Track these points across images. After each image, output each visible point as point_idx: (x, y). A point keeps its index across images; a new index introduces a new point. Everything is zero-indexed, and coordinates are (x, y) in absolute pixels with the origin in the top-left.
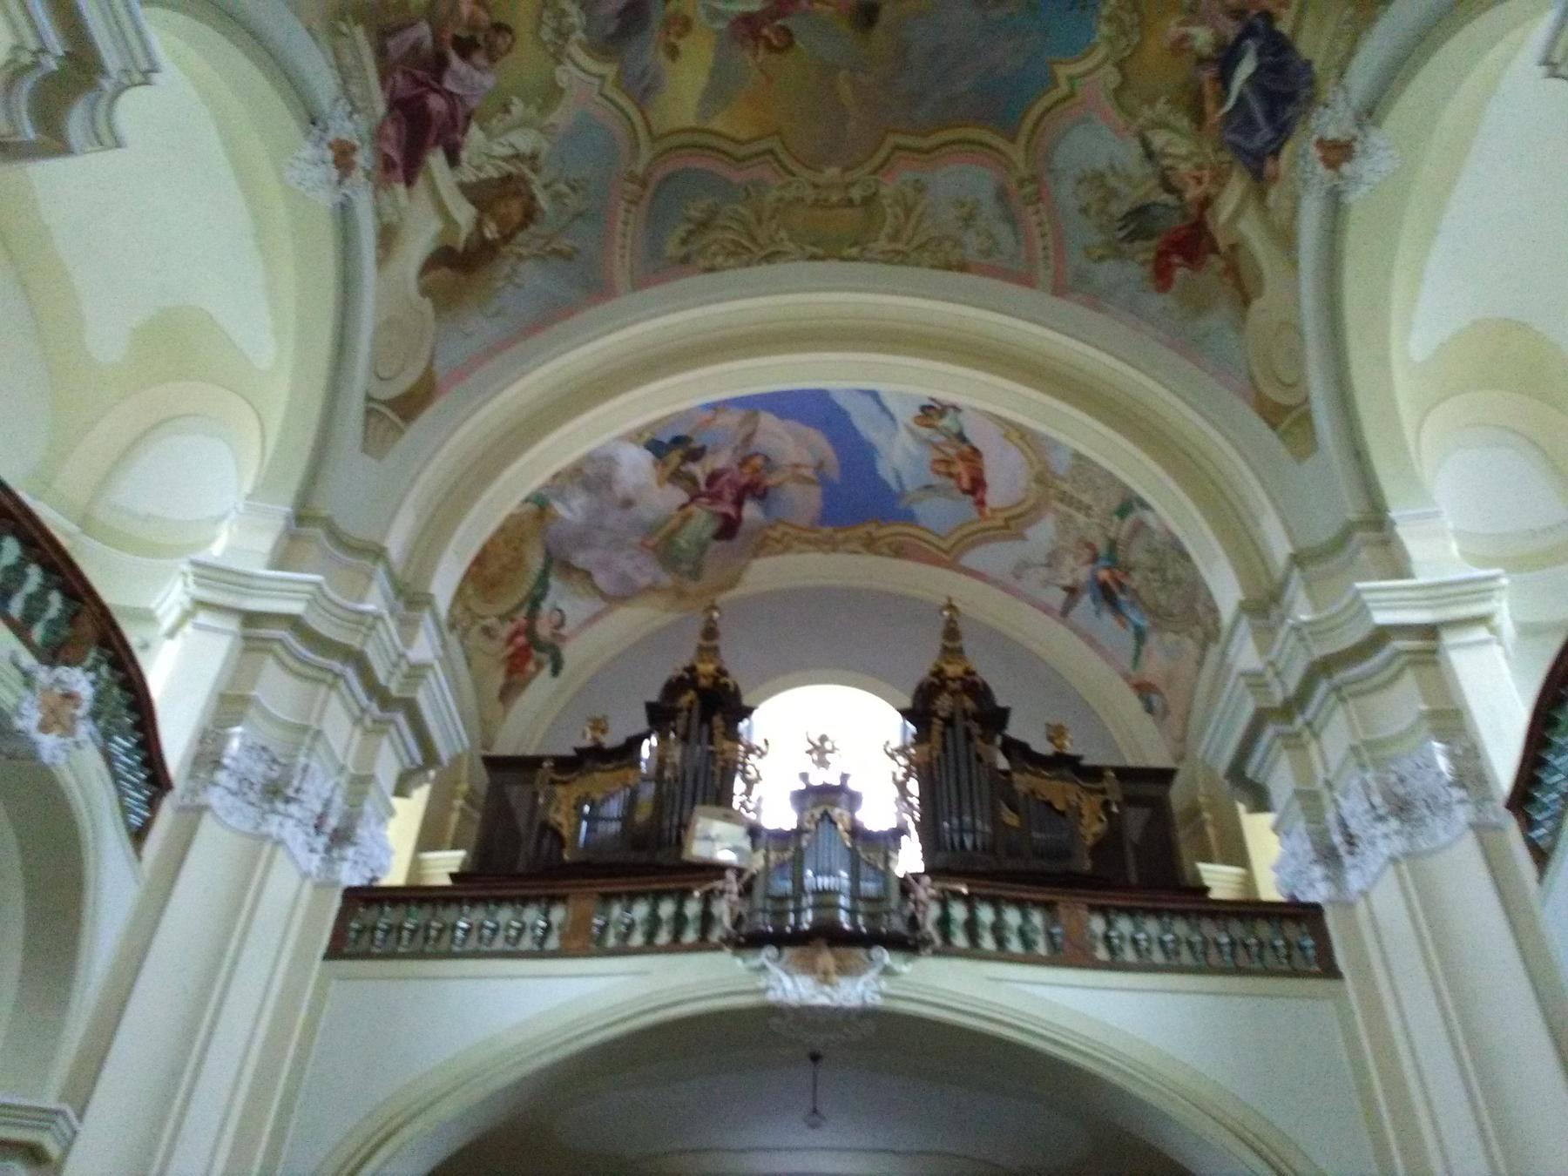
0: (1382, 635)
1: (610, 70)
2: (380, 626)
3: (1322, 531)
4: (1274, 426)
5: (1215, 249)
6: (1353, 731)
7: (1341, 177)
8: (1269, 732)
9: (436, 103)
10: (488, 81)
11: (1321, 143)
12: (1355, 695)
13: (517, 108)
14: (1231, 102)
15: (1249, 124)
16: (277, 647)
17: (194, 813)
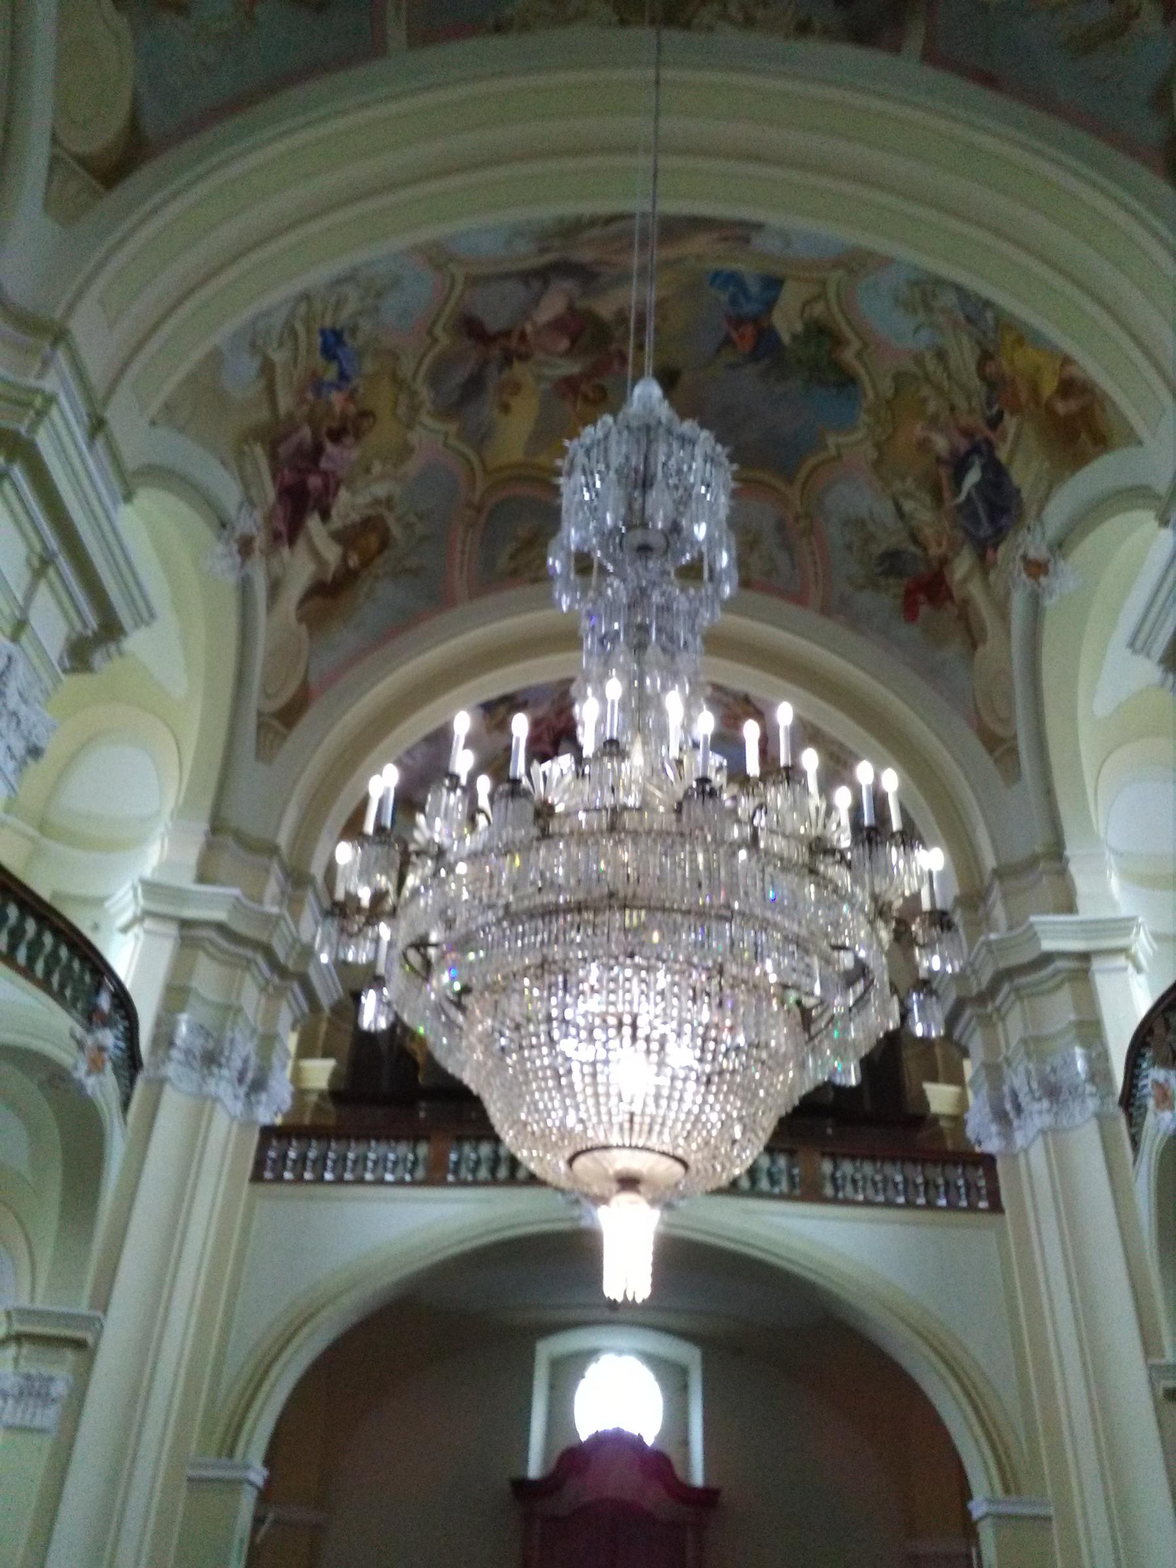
0: (1047, 958)
1: (453, 427)
2: (282, 923)
3: (1019, 852)
4: (991, 751)
5: (950, 596)
6: (1026, 1027)
7: (1039, 584)
8: (968, 1013)
9: (314, 482)
10: (354, 454)
11: (1024, 557)
12: (1028, 996)
13: (377, 468)
14: (963, 497)
15: (974, 517)
16: (207, 945)
17: (160, 1083)
